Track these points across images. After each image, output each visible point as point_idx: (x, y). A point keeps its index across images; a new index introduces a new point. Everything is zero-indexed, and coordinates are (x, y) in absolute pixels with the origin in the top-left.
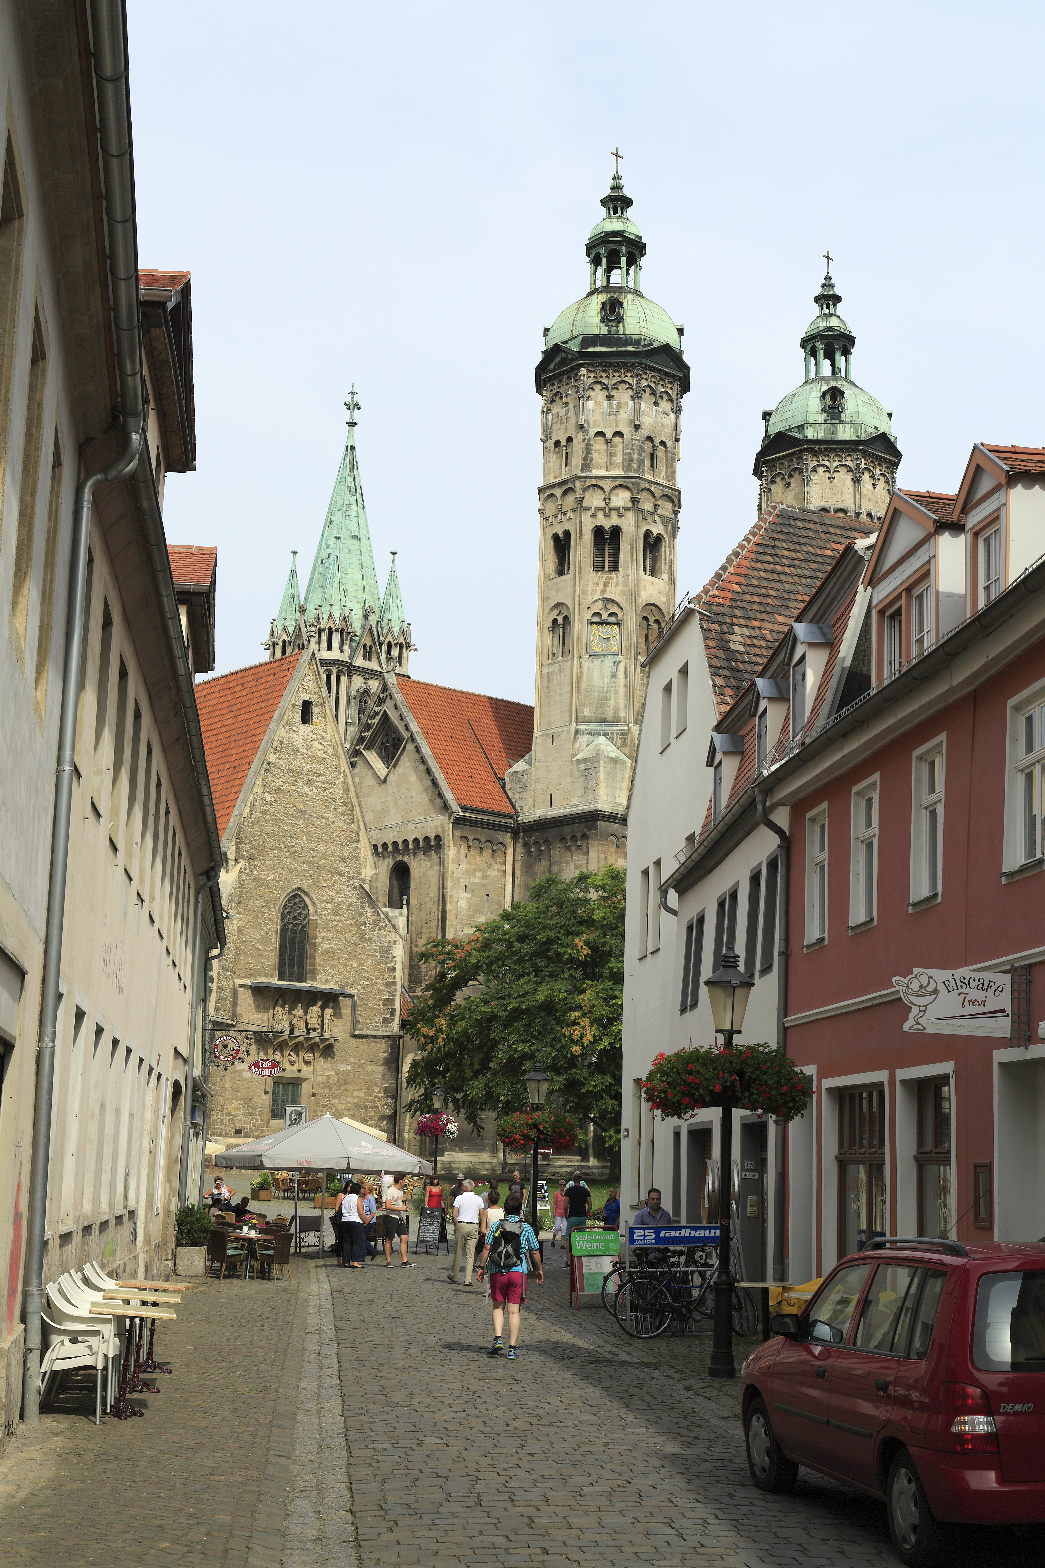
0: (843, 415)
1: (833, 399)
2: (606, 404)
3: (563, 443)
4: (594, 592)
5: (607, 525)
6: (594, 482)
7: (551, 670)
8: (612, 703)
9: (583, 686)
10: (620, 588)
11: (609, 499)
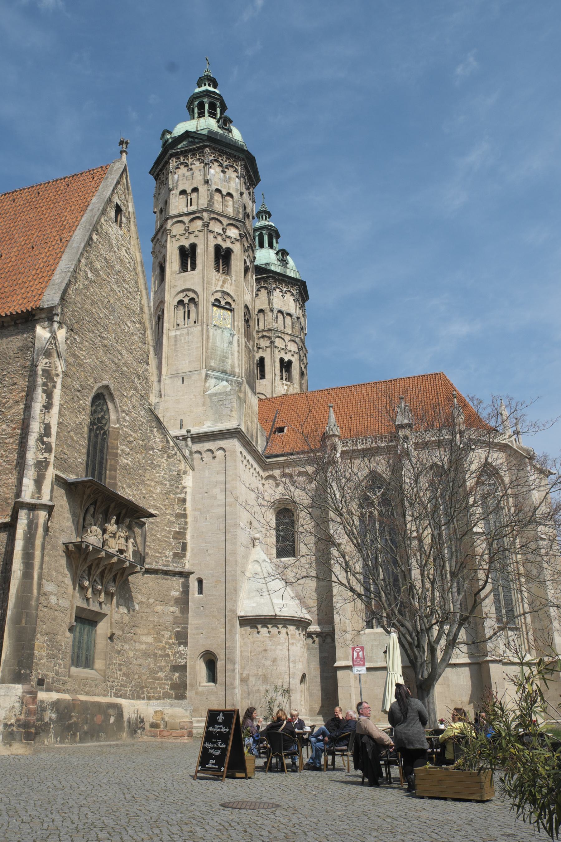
1: (283, 256)
4: (216, 285)
5: (224, 246)
6: (216, 216)
8: (230, 361)
9: (210, 345)
10: (233, 287)
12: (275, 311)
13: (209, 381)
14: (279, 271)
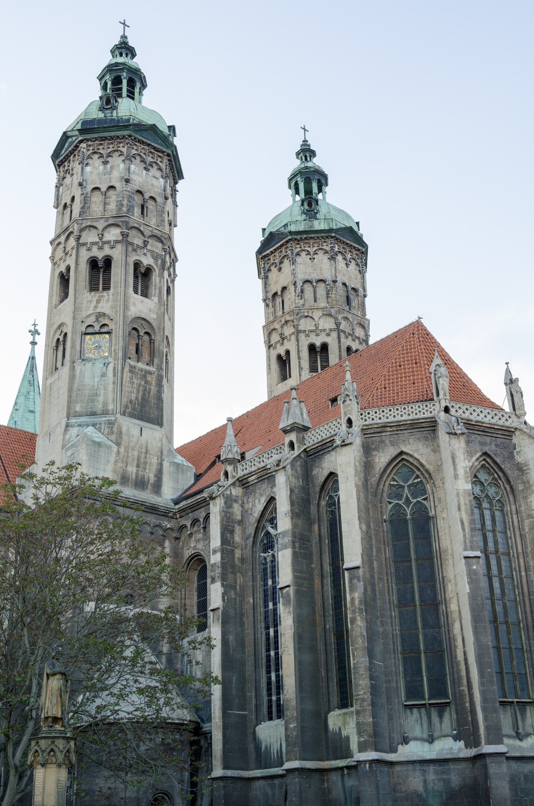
0: (318, 216)
1: (310, 205)
2: (101, 168)
3: (69, 203)
4: (87, 308)
5: (100, 255)
6: (89, 223)
7: (52, 380)
8: (101, 399)
9: (76, 386)
10: (110, 304)
11: (102, 235)
12: (299, 284)
13: (69, 432)
14: (302, 228)
